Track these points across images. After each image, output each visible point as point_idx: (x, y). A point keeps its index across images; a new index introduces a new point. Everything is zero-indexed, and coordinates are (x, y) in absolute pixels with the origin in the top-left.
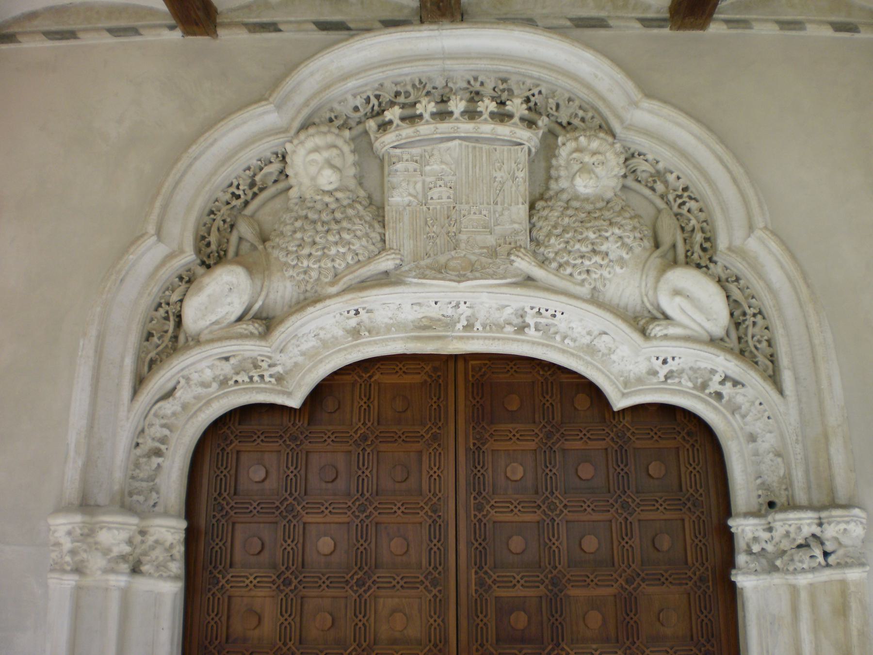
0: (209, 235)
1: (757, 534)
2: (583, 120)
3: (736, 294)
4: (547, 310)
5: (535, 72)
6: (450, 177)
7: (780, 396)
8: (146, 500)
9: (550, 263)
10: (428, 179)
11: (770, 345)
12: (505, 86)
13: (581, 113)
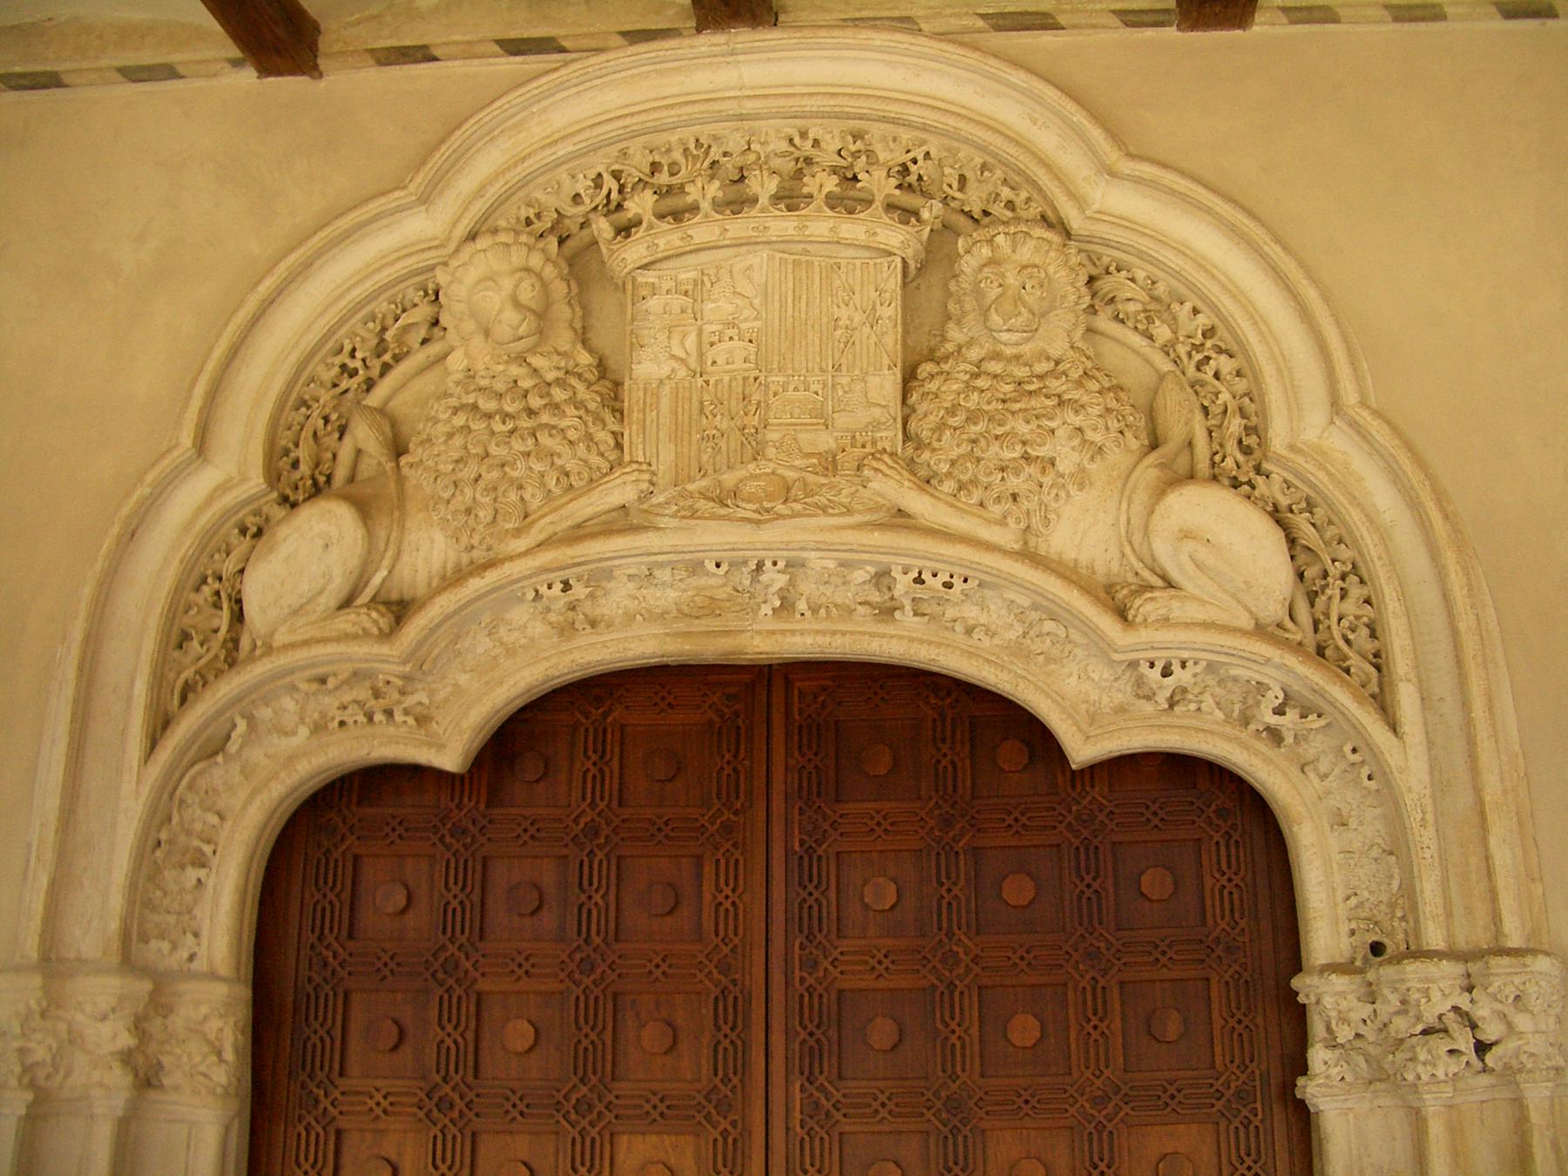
0: (297, 445)
1: (1344, 1005)
2: (1010, 205)
3: (1308, 534)
4: (935, 575)
5: (915, 114)
6: (749, 325)
7: (1390, 735)
8: (174, 948)
9: (941, 481)
10: (709, 328)
11: (1373, 635)
12: (859, 145)
13: (1006, 193)
